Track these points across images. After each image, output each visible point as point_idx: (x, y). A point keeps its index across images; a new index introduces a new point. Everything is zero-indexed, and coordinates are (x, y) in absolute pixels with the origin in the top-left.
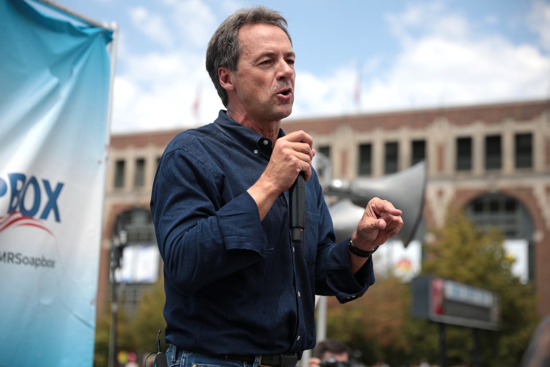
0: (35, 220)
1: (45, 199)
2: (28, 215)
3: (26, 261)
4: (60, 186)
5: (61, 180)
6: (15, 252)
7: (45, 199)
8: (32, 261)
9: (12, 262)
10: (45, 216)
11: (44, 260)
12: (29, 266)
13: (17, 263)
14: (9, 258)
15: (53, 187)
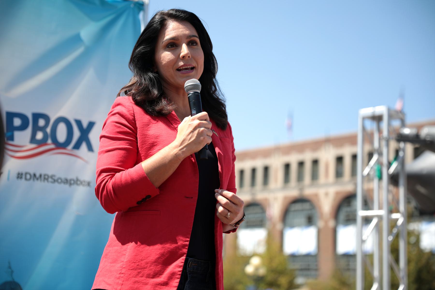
0: (69, 150)
1: (77, 134)
2: (63, 146)
3: (60, 181)
4: (91, 125)
5: (93, 120)
6: (50, 174)
7: (77, 134)
8: (66, 181)
9: (48, 181)
10: (77, 146)
11: (78, 180)
12: (62, 185)
13: (52, 182)
14: (45, 178)
15: (85, 124)
